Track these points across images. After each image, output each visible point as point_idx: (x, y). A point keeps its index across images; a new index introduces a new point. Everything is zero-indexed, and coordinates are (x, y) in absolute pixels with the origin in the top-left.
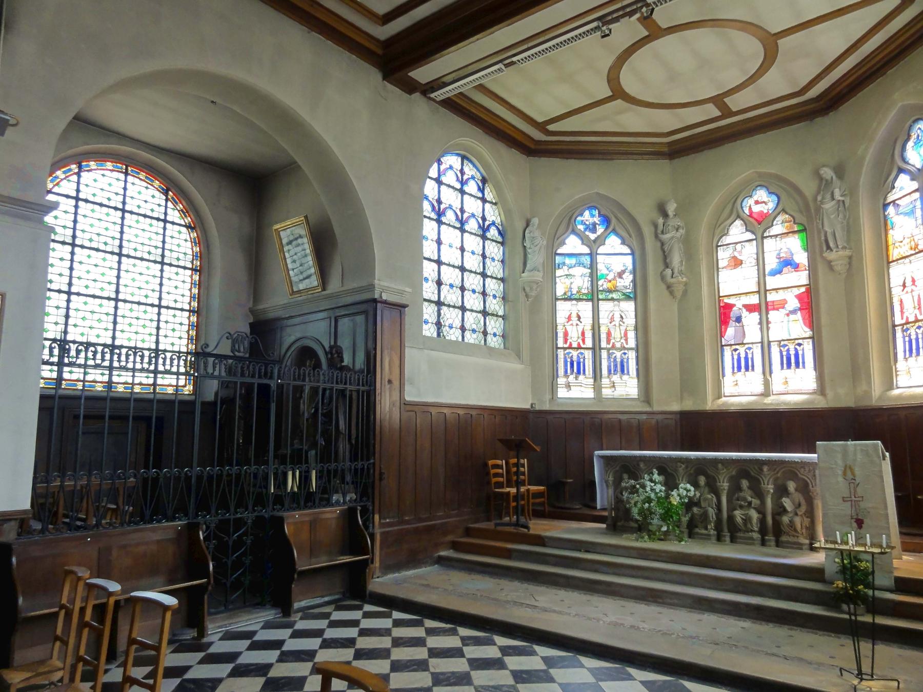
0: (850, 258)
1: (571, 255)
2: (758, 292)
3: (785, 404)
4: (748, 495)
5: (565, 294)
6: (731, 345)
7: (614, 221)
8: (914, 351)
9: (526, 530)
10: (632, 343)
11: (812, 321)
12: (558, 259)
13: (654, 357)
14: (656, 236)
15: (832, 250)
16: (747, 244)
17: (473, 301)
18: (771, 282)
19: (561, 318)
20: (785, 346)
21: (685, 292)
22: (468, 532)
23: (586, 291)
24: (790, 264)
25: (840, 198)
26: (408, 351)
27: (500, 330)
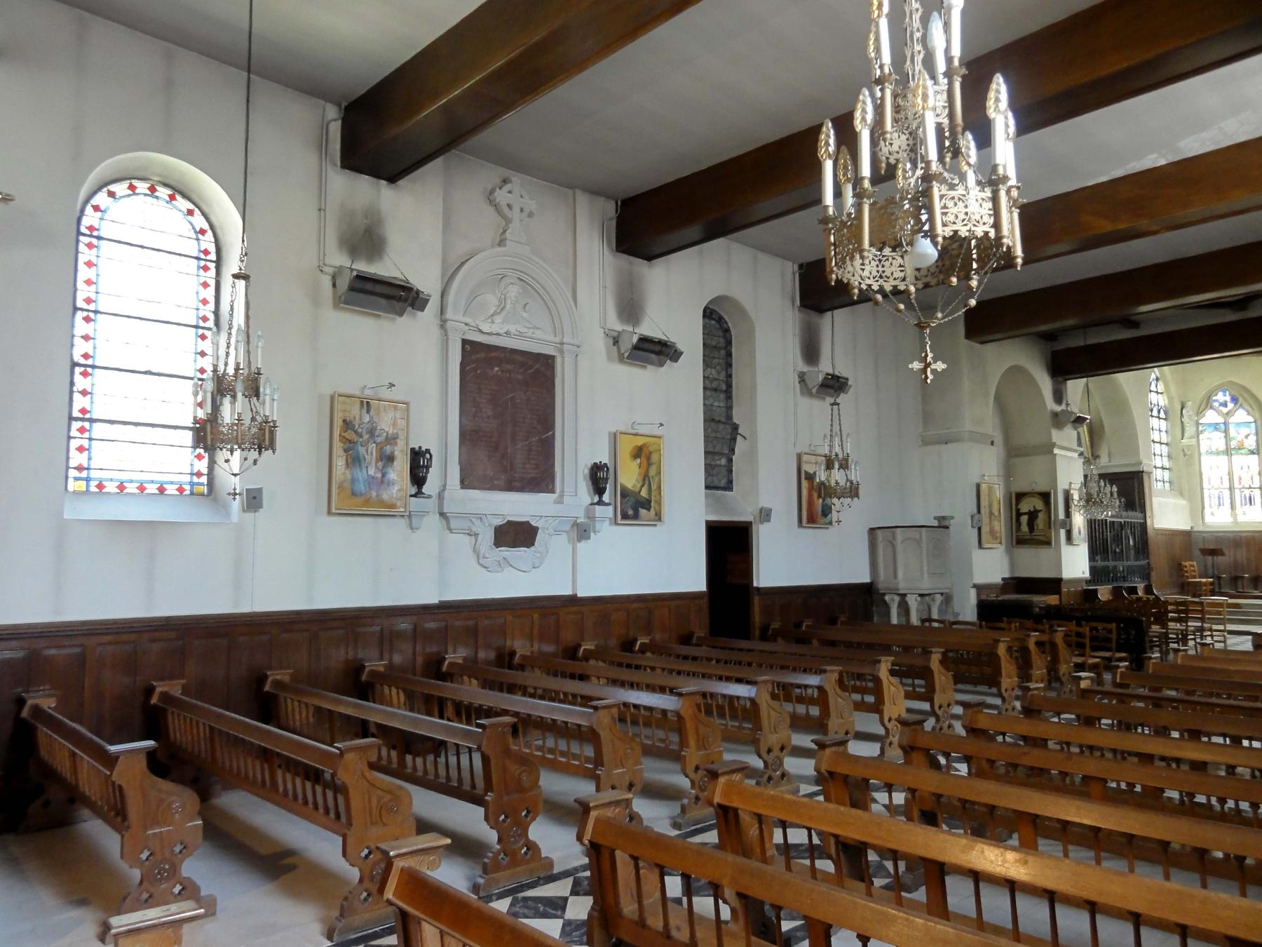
1: (1210, 425)
7: (1241, 400)
10: (1257, 484)
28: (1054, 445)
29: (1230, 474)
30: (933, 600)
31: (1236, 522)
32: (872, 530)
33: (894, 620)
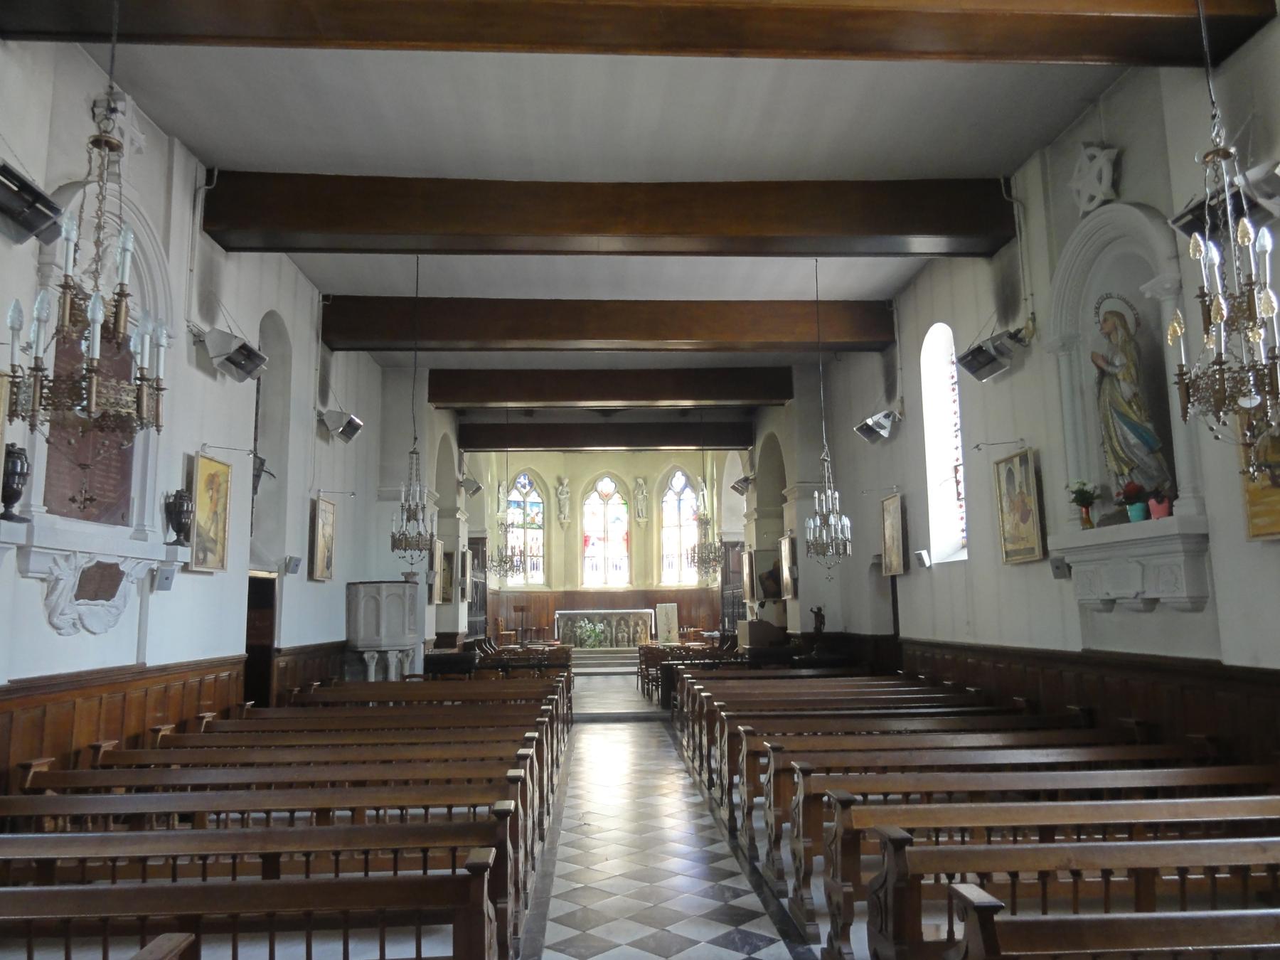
4: (623, 626)
13: (554, 560)
28: (457, 509)
30: (407, 656)
31: (527, 584)
32: (349, 584)
33: (372, 678)
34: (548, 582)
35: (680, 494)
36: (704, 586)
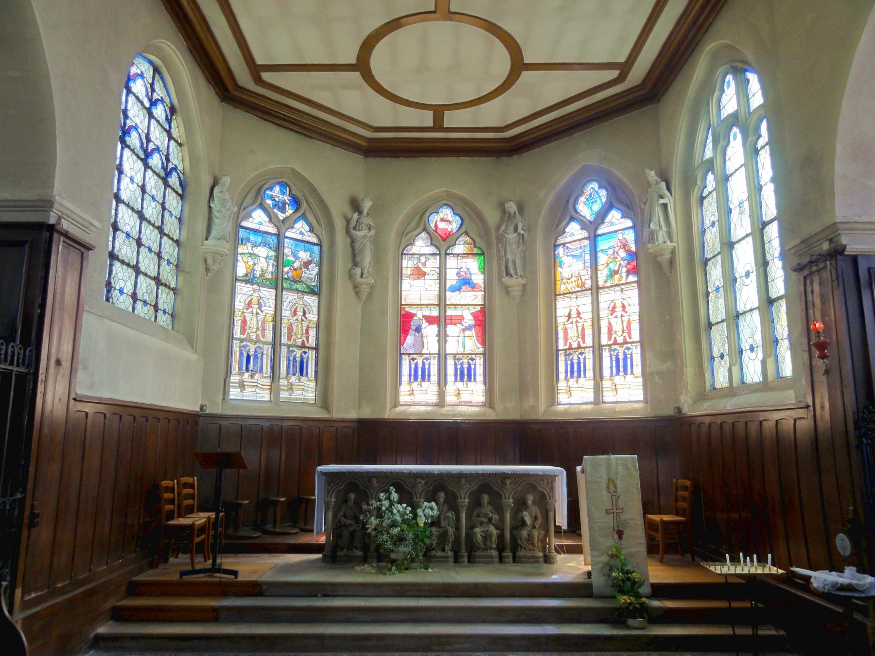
0: (524, 286)
1: (256, 231)
2: (439, 305)
3: (460, 414)
4: (487, 509)
5: (246, 275)
6: (409, 354)
7: (304, 205)
8: (575, 373)
9: (233, 577)
10: (312, 342)
11: (484, 338)
12: (242, 233)
14: (348, 232)
15: (511, 276)
16: (431, 257)
17: (148, 263)
18: (452, 297)
19: (239, 305)
20: (459, 359)
21: (370, 295)
22: (135, 589)
23: (270, 277)
24: (469, 284)
25: (522, 232)
26: (86, 318)
27: (170, 307)
29: (277, 319)
34: (325, 397)
35: (592, 228)
36: (670, 411)
